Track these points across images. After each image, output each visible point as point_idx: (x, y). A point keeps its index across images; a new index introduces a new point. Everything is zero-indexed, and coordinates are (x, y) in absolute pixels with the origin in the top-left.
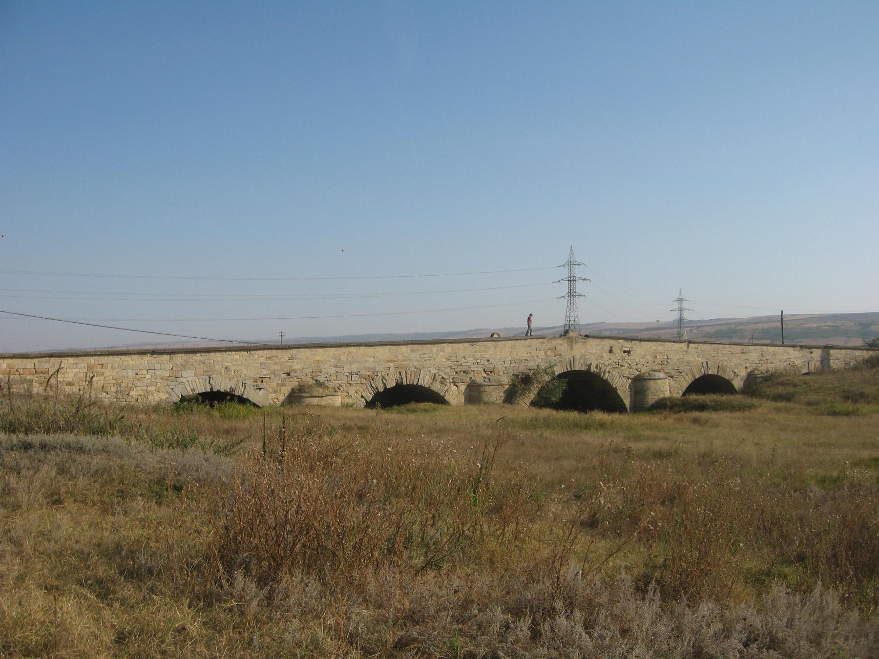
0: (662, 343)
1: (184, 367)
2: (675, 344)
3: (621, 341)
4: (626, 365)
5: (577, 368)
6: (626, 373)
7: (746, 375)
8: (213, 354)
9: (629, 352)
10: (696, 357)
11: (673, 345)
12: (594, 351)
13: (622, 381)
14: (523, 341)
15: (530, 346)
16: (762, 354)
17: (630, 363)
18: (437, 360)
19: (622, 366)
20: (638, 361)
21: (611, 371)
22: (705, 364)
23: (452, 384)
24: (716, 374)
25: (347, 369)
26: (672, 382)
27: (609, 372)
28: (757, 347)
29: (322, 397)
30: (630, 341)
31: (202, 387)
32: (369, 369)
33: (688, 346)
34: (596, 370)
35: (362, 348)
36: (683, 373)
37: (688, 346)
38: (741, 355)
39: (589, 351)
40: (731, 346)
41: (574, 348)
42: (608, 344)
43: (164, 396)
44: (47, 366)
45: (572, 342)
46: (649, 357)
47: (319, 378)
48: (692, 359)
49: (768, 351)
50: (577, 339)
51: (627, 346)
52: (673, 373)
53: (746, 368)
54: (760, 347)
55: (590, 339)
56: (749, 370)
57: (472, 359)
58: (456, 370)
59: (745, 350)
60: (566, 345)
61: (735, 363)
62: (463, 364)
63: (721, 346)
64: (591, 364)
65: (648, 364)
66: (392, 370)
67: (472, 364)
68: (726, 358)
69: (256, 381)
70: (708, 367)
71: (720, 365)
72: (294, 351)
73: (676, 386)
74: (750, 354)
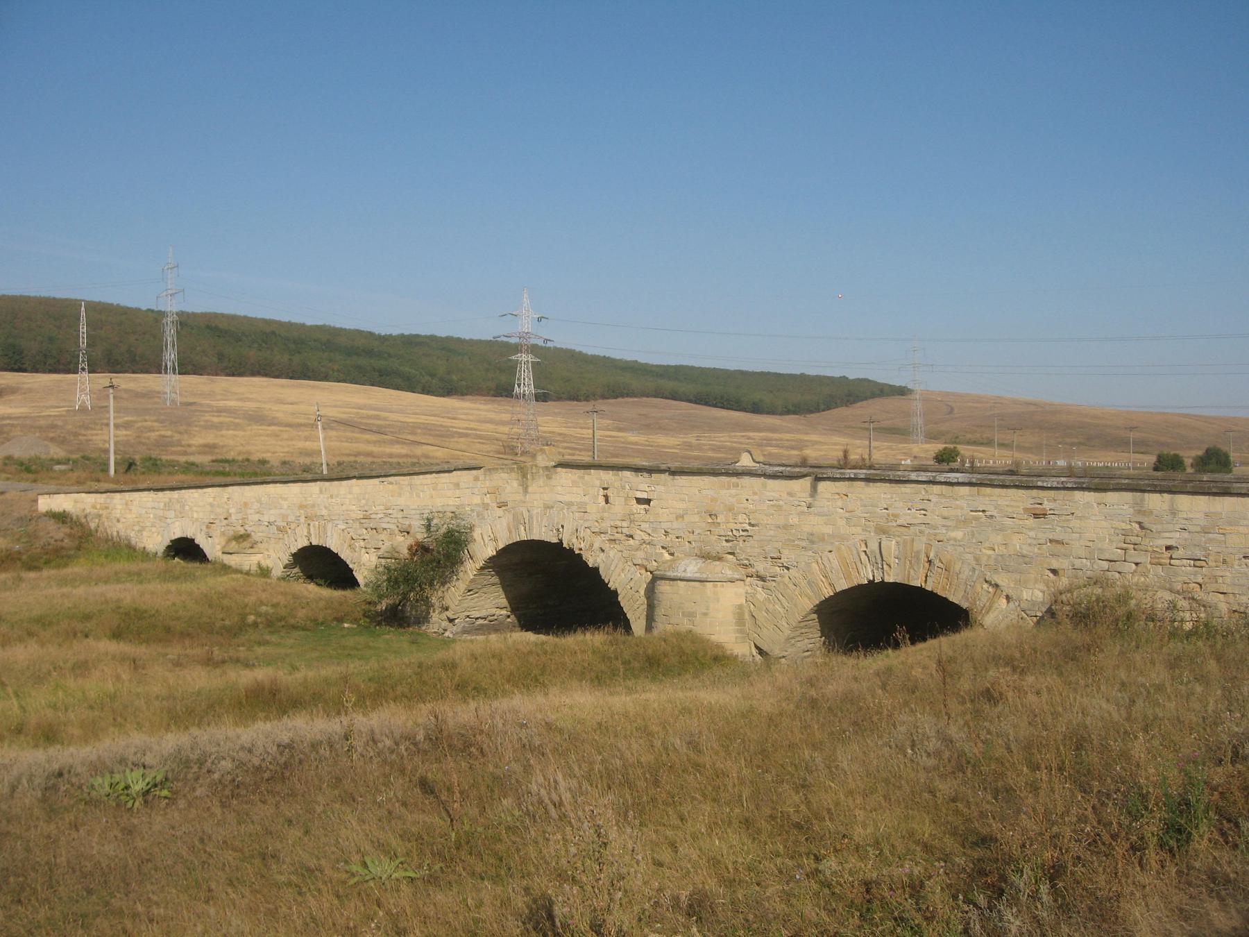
0: (734, 480)
1: (168, 506)
2: (771, 482)
3: (627, 474)
4: (639, 535)
5: (536, 536)
6: (640, 557)
7: (1047, 599)
8: (183, 491)
9: (648, 501)
10: (842, 523)
11: (764, 486)
12: (567, 498)
13: (629, 576)
14: (447, 474)
15: (457, 485)
16: (1142, 528)
17: (650, 532)
18: (344, 507)
19: (631, 536)
20: (665, 526)
21: (606, 546)
22: (874, 546)
23: (363, 550)
24: (917, 582)
25: (266, 519)
26: (761, 595)
27: (603, 551)
28: (1109, 494)
29: (231, 554)
30: (645, 474)
31: (178, 531)
32: (284, 517)
33: (814, 489)
34: (574, 540)
35: (278, 485)
36: (793, 572)
37: (814, 489)
38: (1031, 522)
39: (560, 498)
40: (983, 489)
41: (530, 489)
42: (598, 483)
43: (159, 539)
44: (108, 501)
45: (524, 476)
46: (697, 518)
47: (247, 527)
48: (828, 530)
49: (1173, 512)
50: (534, 471)
51: (642, 485)
52: (761, 567)
53: (1054, 572)
54: (1128, 496)
55: (559, 469)
56: (1064, 582)
57: (382, 508)
58: (366, 526)
59: (1047, 505)
60: (515, 484)
61: (1001, 550)
62: (373, 516)
63: (936, 489)
64: (563, 526)
65: (691, 537)
66: (302, 519)
67: (382, 516)
68: (958, 534)
69: (207, 527)
70: (882, 560)
71: (932, 556)
72: (230, 489)
73: (771, 607)
74: (1075, 523)
